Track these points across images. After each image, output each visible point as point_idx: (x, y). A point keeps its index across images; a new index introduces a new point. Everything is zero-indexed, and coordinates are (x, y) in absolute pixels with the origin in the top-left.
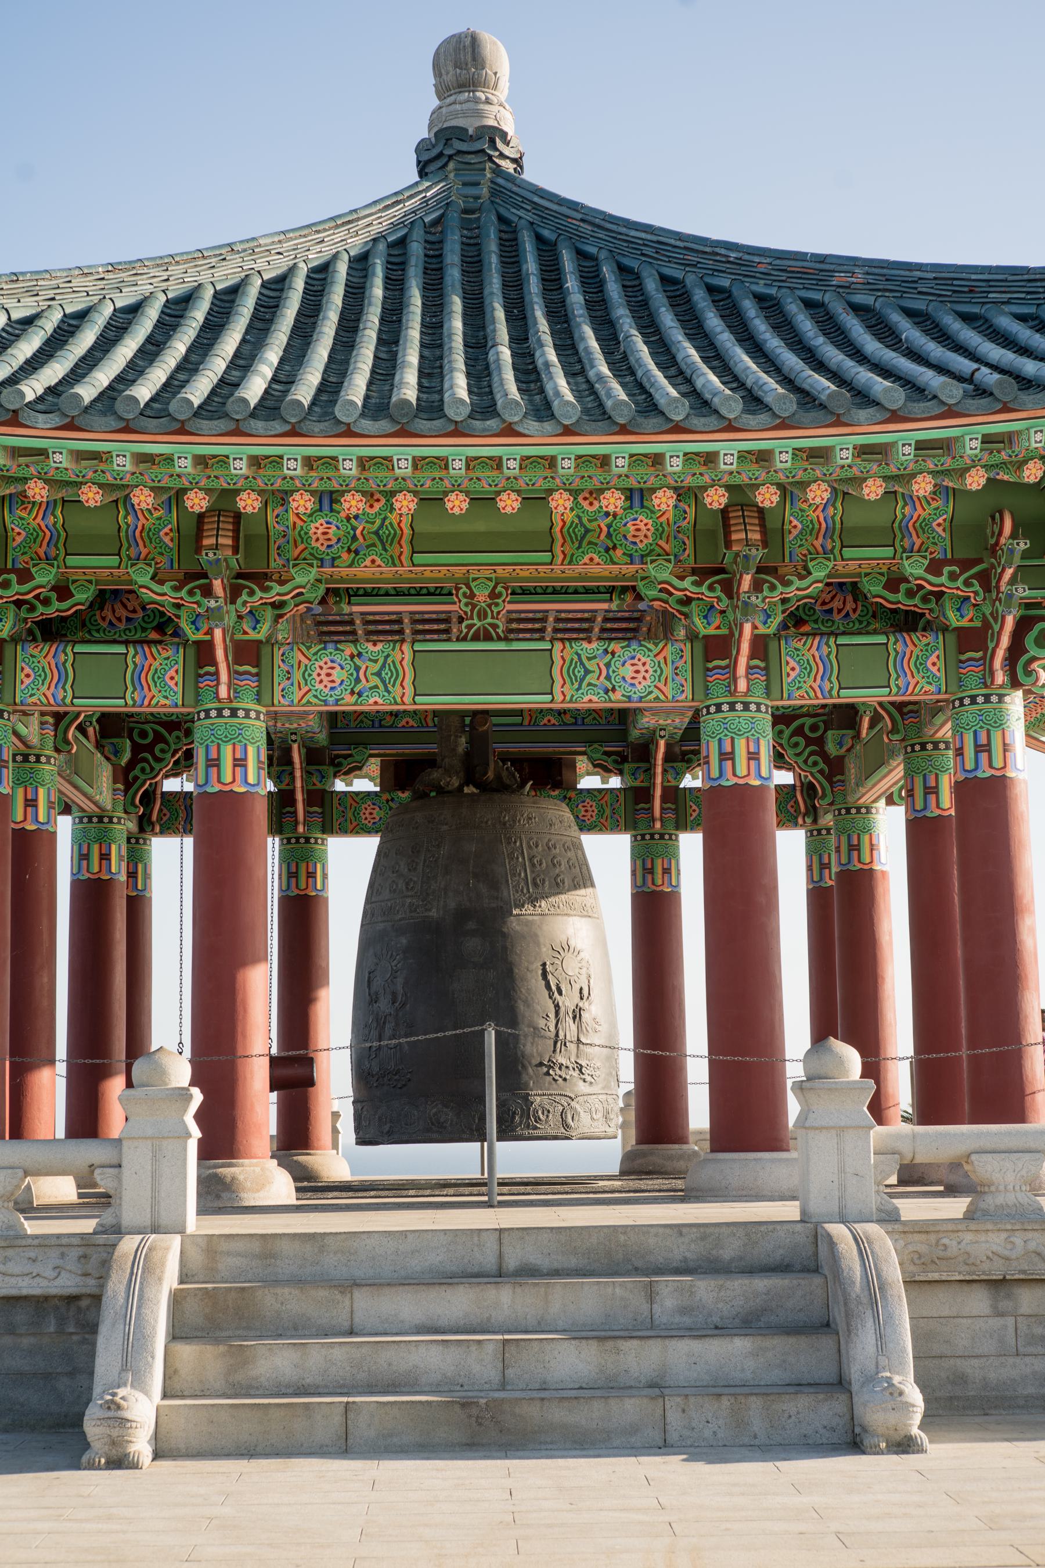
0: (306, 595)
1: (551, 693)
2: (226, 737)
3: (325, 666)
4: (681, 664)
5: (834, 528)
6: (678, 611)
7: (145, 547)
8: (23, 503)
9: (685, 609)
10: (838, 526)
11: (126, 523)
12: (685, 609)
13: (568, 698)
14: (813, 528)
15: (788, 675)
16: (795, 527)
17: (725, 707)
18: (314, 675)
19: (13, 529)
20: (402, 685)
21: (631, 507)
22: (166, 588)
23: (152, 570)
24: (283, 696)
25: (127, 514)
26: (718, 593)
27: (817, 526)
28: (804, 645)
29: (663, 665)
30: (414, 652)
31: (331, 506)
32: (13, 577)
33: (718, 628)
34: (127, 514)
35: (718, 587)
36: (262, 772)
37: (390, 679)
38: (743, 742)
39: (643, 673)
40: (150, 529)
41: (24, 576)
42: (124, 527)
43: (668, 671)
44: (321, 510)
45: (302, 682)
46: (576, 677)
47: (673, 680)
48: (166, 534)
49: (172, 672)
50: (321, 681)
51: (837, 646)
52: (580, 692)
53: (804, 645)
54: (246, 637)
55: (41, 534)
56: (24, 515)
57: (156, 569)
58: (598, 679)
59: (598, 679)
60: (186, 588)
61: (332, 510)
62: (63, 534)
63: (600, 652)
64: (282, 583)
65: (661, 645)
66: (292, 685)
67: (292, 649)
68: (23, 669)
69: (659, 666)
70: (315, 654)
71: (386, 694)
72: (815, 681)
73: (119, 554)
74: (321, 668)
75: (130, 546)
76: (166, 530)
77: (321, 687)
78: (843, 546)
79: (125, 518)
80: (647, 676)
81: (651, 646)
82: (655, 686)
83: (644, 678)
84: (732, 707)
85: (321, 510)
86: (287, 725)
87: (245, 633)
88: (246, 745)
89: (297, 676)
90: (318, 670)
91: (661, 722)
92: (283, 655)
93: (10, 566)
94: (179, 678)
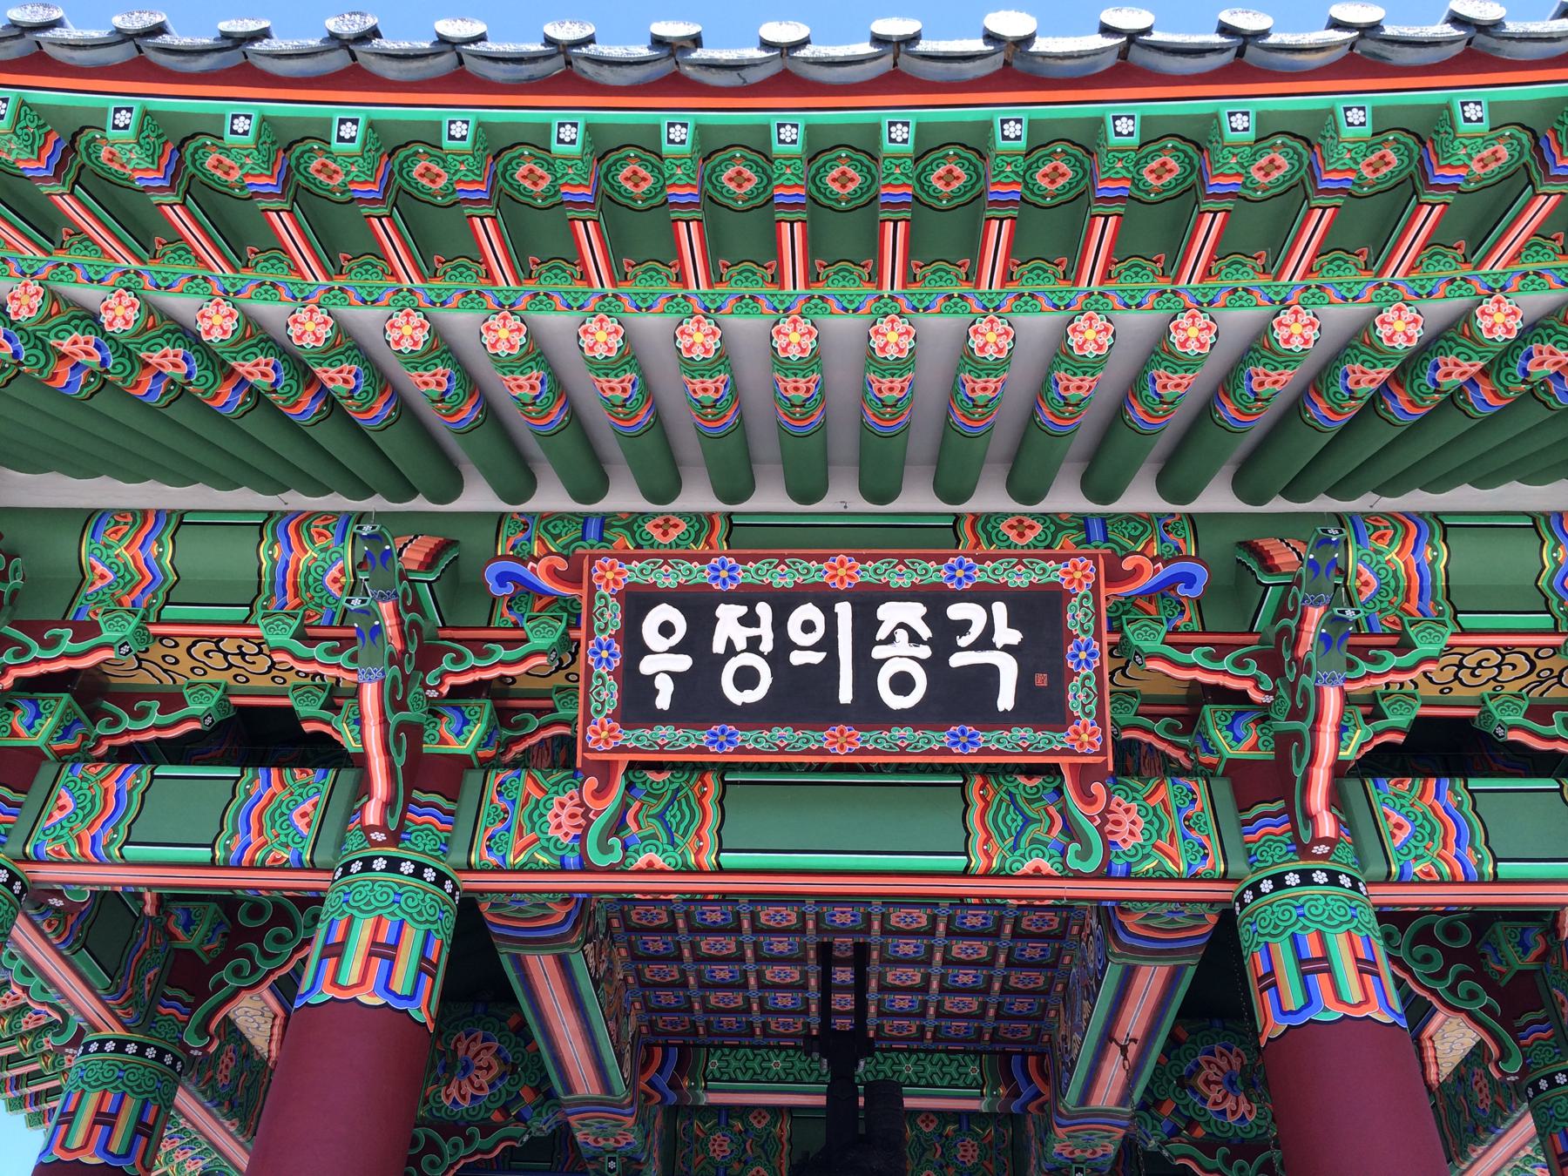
0: (561, 712)
1: (966, 853)
2: (369, 903)
3: (569, 803)
4: (1193, 811)
5: (1434, 587)
6: (1170, 743)
7: (296, 596)
8: (117, 523)
9: (1185, 740)
10: (1441, 583)
11: (271, 557)
12: (1185, 740)
13: (995, 864)
14: (1397, 587)
15: (1393, 836)
16: (1366, 584)
17: (1292, 879)
18: (549, 816)
19: (93, 568)
20: (698, 834)
21: (1088, 541)
22: (317, 651)
23: (295, 623)
24: (489, 847)
25: (275, 541)
26: (1253, 669)
27: (1403, 584)
28: (1410, 790)
29: (1161, 812)
30: (725, 784)
31: (601, 532)
32: (68, 633)
33: (1255, 748)
34: (275, 541)
35: (1253, 663)
36: (427, 980)
37: (678, 824)
38: (1343, 939)
39: (1127, 826)
40: (308, 572)
41: (86, 630)
42: (266, 564)
43: (1174, 823)
44: (583, 538)
45: (527, 825)
46: (1009, 828)
47: (1185, 838)
48: (335, 580)
49: (307, 807)
50: (559, 826)
51: (1471, 792)
52: (1018, 853)
53: (1410, 790)
54: (443, 749)
55: (138, 577)
56: (111, 540)
57: (302, 626)
58: (1049, 832)
59: (1049, 832)
60: (349, 651)
61: (601, 539)
62: (172, 578)
63: (1050, 790)
64: (510, 644)
65: (1153, 783)
66: (508, 830)
67: (519, 777)
68: (59, 797)
69: (1155, 814)
70: (557, 784)
71: (670, 848)
72: (1445, 847)
73: (251, 606)
74: (562, 805)
75: (272, 594)
76: (334, 572)
77: (559, 834)
78: (1456, 612)
79: (271, 548)
80: (1137, 830)
81: (1135, 783)
82: (1154, 846)
83: (1132, 833)
84: (1306, 878)
85: (583, 538)
86: (602, 1143)
87: (443, 741)
88: (402, 922)
89: (519, 816)
90: (556, 809)
91: (1078, 1153)
92: (500, 785)
93: (70, 617)
94: (316, 817)
